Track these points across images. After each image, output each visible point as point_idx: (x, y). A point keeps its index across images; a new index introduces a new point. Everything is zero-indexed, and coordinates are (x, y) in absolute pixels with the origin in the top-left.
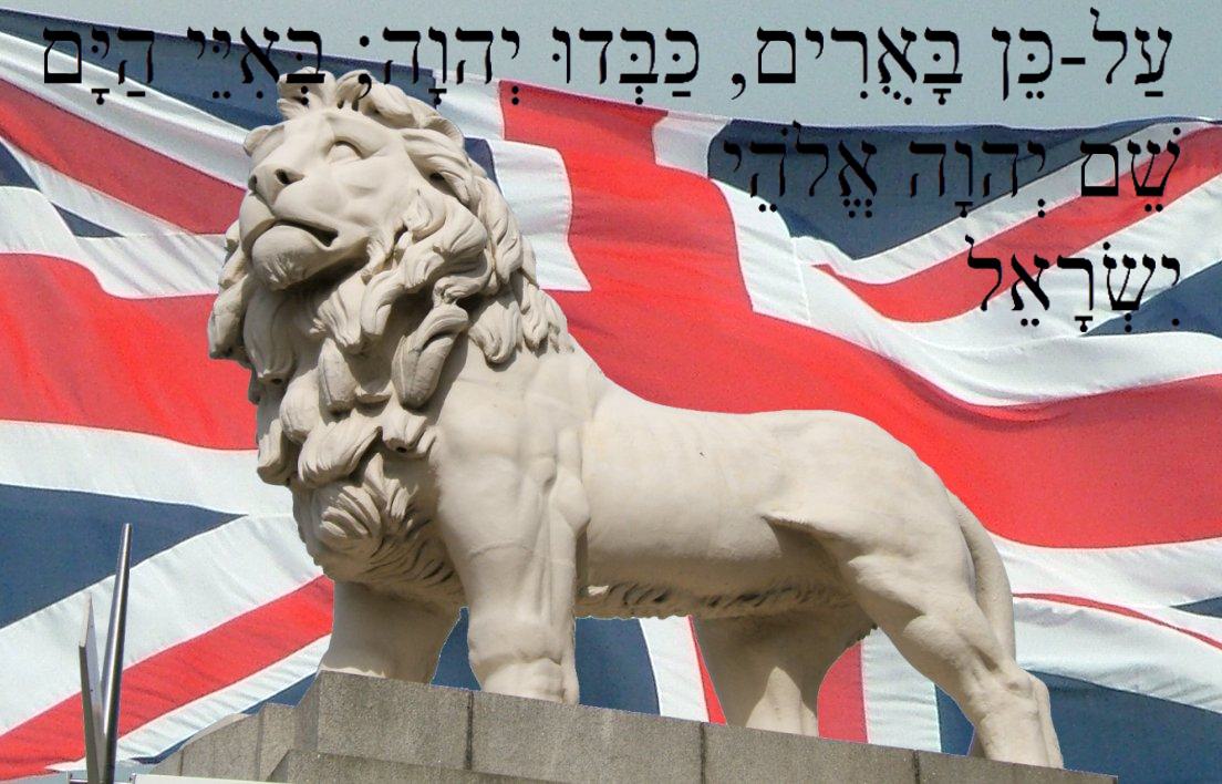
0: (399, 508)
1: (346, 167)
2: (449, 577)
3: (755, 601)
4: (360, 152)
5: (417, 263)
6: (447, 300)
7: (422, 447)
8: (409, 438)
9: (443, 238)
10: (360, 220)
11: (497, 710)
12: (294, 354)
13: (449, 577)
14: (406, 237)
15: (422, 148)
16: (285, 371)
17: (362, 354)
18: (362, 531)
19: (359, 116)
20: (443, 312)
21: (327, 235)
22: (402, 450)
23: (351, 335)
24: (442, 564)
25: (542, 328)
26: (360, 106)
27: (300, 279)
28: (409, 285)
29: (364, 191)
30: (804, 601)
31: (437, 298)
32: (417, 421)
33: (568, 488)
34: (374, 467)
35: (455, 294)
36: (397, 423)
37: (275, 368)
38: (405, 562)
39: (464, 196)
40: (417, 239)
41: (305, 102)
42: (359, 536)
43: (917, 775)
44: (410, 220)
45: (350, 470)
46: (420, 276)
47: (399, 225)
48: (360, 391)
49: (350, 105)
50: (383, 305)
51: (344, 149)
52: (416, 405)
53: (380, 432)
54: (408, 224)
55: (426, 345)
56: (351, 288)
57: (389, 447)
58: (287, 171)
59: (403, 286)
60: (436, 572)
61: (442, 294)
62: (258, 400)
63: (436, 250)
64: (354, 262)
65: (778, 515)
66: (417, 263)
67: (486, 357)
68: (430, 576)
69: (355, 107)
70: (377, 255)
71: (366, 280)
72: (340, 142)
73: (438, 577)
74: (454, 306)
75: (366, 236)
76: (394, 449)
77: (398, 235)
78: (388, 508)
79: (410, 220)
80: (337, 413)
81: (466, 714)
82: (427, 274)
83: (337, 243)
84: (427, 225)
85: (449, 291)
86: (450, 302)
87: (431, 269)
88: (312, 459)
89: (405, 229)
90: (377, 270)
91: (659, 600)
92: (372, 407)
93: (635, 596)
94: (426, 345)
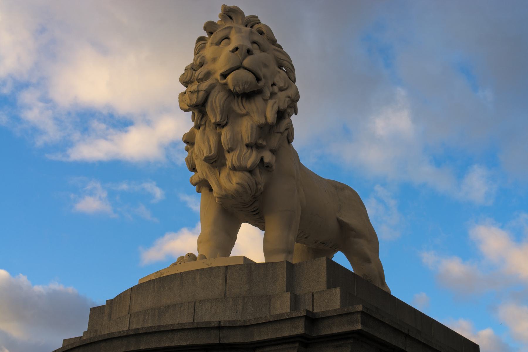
0: (261, 187)
2: (257, 214)
13: (257, 214)
14: (276, 89)
16: (225, 122)
17: (262, 128)
18: (250, 192)
21: (258, 79)
34: (258, 172)
36: (268, 157)
37: (222, 120)
40: (281, 90)
41: (231, 18)
44: (277, 82)
48: (260, 141)
49: (250, 27)
52: (273, 152)
54: (276, 83)
56: (259, 101)
62: (199, 128)
63: (289, 97)
65: (341, 218)
66: (285, 100)
68: (250, 212)
71: (266, 101)
73: (255, 213)
79: (277, 82)
88: (231, 159)
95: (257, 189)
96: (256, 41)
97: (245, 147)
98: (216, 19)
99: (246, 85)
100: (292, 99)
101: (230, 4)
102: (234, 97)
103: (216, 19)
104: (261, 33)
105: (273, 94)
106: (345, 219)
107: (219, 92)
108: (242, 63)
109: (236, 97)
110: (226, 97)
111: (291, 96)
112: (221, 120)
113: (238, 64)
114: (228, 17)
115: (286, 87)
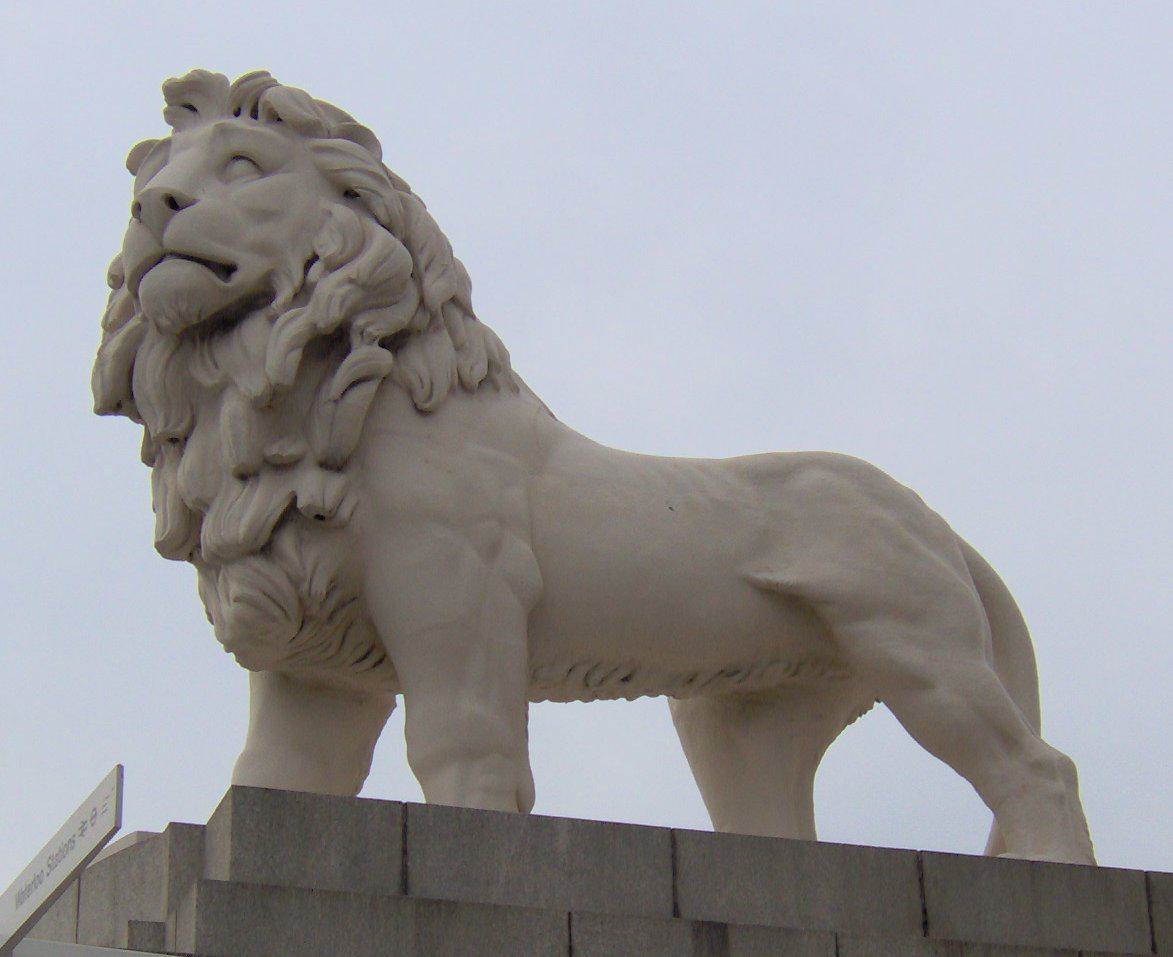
1: (248, 188)
2: (381, 661)
3: (737, 677)
4: (260, 168)
5: (331, 294)
6: (367, 340)
7: (345, 512)
8: (329, 504)
9: (360, 266)
10: (263, 249)
11: (323, 917)
12: (192, 409)
13: (381, 661)
14: (317, 268)
15: (336, 162)
17: (270, 407)
18: (277, 612)
19: (262, 128)
20: (364, 354)
21: (227, 270)
22: (320, 517)
23: (253, 384)
24: (373, 648)
25: (480, 370)
26: (260, 113)
27: (195, 321)
28: (321, 325)
29: (265, 215)
30: (796, 673)
31: (355, 340)
32: (336, 483)
33: (518, 549)
34: (287, 542)
35: (376, 334)
36: (312, 487)
37: (168, 428)
38: (330, 645)
39: (384, 219)
40: (333, 266)
41: (192, 108)
42: (274, 619)
43: (921, 880)
45: (262, 542)
46: (336, 315)
47: (309, 255)
48: (273, 450)
50: (292, 350)
51: (240, 166)
52: (332, 465)
53: (294, 499)
54: (319, 252)
55: (344, 394)
56: (253, 329)
57: (306, 514)
58: (174, 196)
59: (315, 325)
60: (365, 657)
61: (362, 333)
62: (154, 462)
63: (351, 281)
64: (258, 299)
65: (763, 576)
66: (331, 297)
67: (415, 406)
69: (254, 115)
70: (284, 294)
71: (272, 320)
72: (237, 157)
73: (368, 663)
74: (376, 348)
75: (271, 267)
76: (311, 517)
77: (309, 264)
78: (306, 586)
79: (321, 246)
80: (243, 477)
81: (399, 829)
82: (344, 310)
83: (237, 278)
84: (341, 253)
85: (370, 329)
86: (370, 343)
87: (348, 303)
89: (315, 258)
90: (287, 307)
91: (626, 679)
92: (283, 467)
93: (597, 676)
94: (344, 394)
95: (300, 600)
96: (243, 152)
97: (237, 485)
98: (164, 131)
99: (180, 304)
100: (360, 283)
101: (180, 74)
102: (195, 345)
103: (164, 131)
104: (276, 119)
105: (304, 292)
106: (787, 573)
107: (152, 346)
108: (161, 245)
109: (198, 344)
110: (167, 355)
111: (354, 276)
112: (166, 426)
113: (152, 249)
114: (186, 110)
115: (349, 249)
